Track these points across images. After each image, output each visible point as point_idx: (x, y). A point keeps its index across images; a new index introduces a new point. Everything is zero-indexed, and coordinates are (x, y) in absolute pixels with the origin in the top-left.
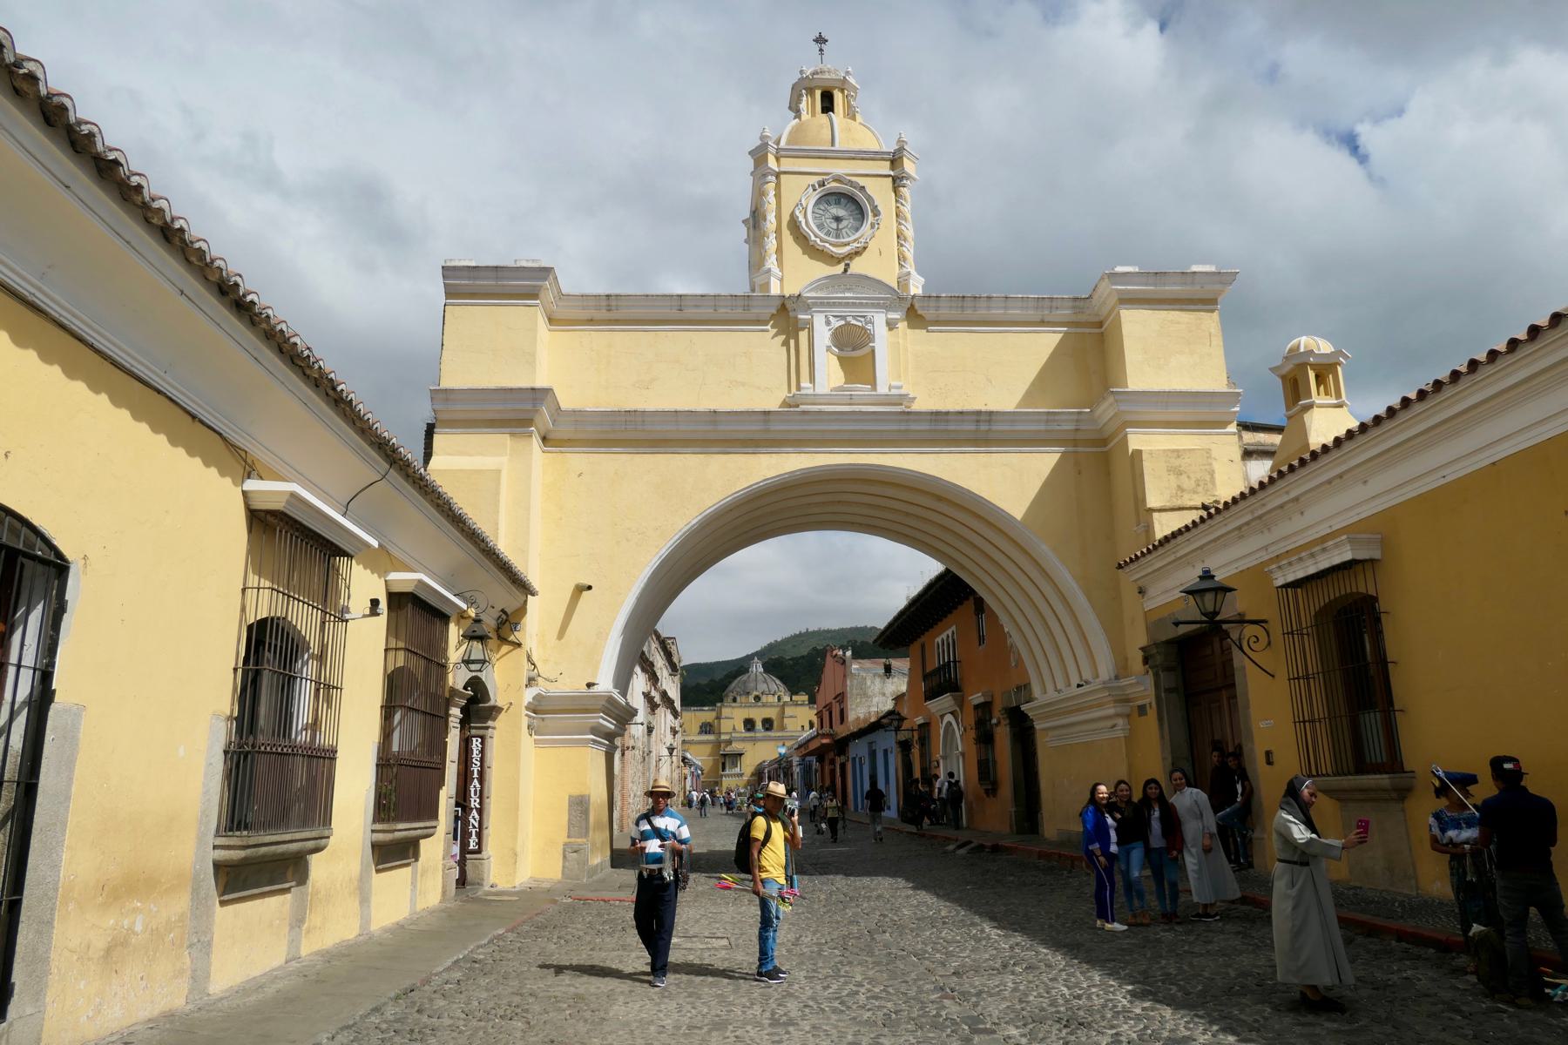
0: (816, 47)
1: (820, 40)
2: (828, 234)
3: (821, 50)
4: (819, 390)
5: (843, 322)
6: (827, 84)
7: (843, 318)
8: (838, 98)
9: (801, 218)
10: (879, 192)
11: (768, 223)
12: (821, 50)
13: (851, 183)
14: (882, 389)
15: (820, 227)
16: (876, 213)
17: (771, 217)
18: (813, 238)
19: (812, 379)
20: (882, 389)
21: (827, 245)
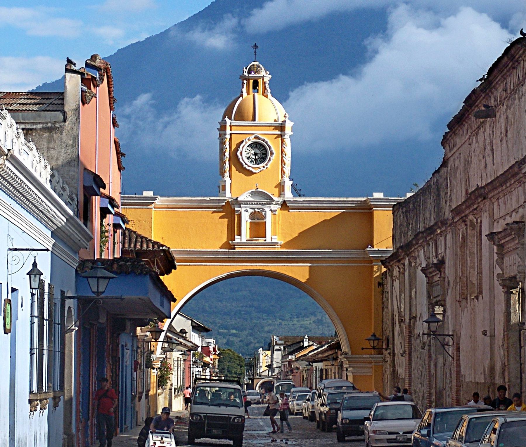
0: (253, 50)
1: (255, 47)
2: (251, 162)
3: (255, 52)
4: (242, 241)
5: (253, 210)
6: (256, 78)
7: (254, 209)
8: (260, 81)
9: (240, 157)
10: (273, 144)
11: (226, 157)
12: (255, 52)
13: (264, 140)
14: (268, 240)
15: (248, 158)
16: (272, 154)
17: (227, 154)
18: (245, 166)
19: (240, 234)
20: (268, 240)
21: (250, 169)
